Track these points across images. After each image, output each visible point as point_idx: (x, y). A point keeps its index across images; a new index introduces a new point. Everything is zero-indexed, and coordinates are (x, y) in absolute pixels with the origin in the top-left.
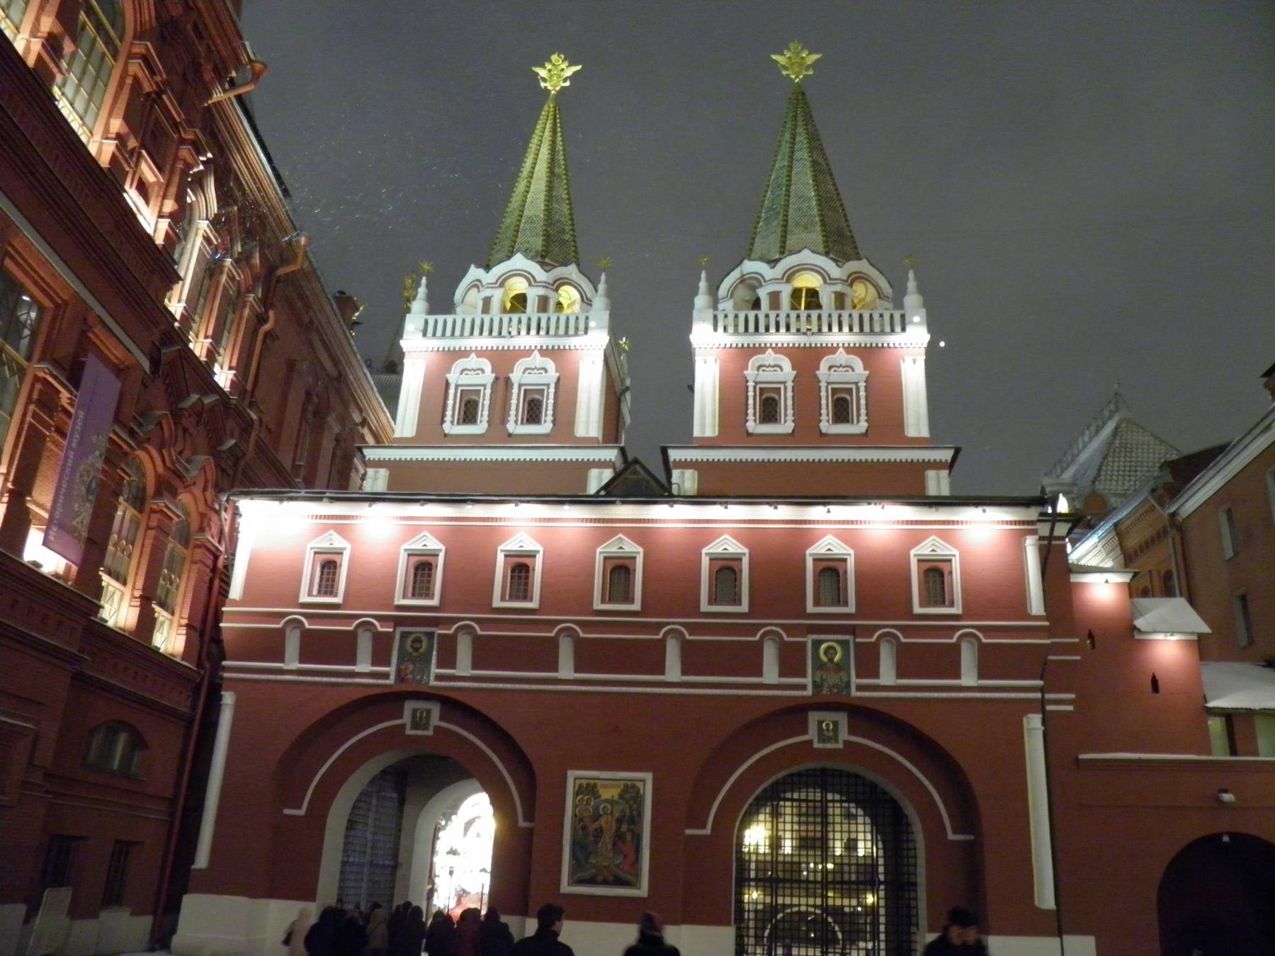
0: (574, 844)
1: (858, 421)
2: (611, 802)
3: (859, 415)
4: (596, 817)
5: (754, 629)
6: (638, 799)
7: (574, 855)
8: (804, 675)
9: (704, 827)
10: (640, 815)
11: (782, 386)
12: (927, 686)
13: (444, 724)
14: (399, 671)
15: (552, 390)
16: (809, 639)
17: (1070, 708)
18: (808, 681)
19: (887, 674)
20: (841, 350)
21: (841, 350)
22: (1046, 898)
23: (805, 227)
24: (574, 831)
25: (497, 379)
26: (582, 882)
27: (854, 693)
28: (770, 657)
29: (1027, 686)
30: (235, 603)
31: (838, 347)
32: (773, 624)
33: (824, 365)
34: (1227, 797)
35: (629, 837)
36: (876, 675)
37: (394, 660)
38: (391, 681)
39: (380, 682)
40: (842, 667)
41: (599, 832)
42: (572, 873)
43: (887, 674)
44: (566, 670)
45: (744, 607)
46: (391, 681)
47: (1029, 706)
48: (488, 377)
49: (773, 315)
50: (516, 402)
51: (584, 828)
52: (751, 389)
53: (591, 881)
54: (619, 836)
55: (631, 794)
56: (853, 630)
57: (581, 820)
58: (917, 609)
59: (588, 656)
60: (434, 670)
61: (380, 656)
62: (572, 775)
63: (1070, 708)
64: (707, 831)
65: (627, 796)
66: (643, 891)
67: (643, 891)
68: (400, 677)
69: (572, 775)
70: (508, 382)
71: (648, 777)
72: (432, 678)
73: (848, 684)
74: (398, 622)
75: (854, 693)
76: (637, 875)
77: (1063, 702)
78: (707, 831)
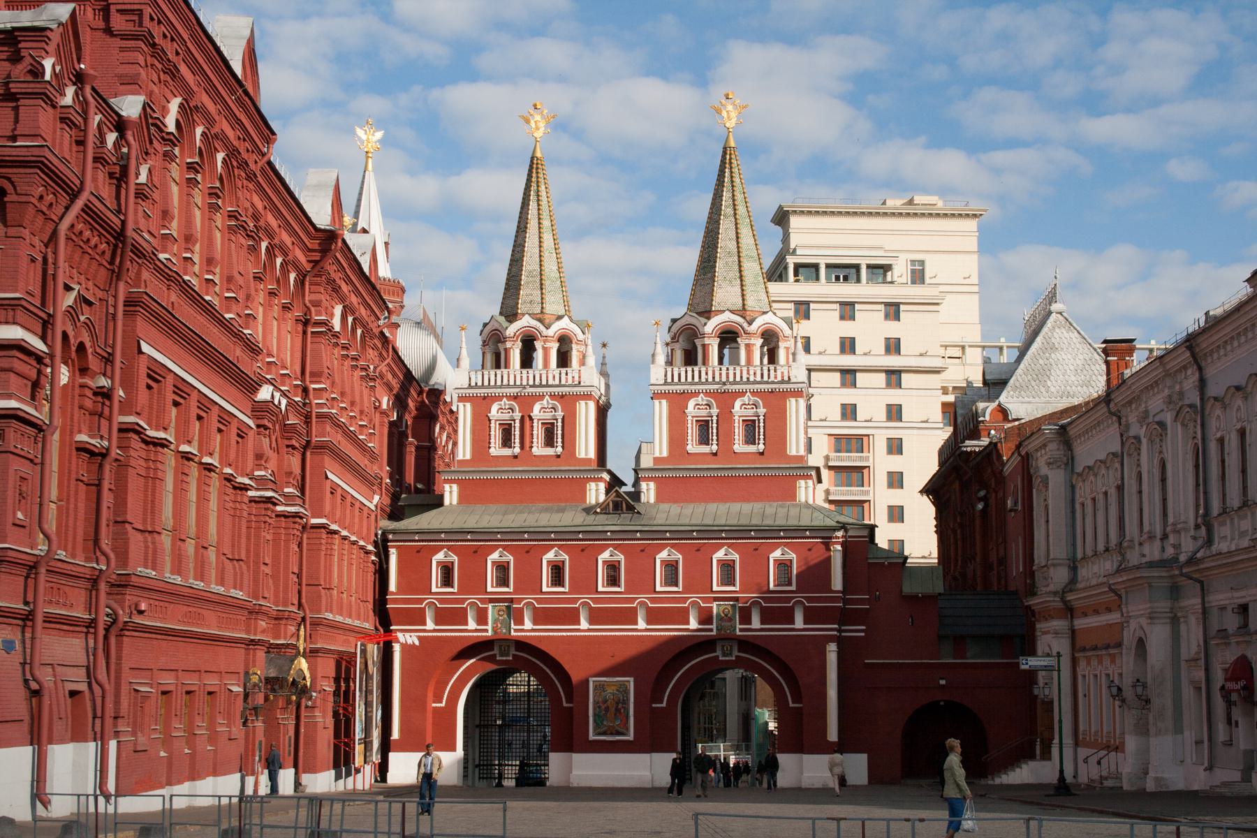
0: (595, 715)
2: (613, 694)
4: (605, 701)
5: (684, 600)
6: (627, 692)
7: (595, 721)
10: (628, 699)
12: (777, 630)
19: (756, 623)
22: (833, 735)
24: (594, 709)
26: (599, 734)
29: (831, 628)
30: (393, 593)
32: (694, 597)
33: (738, 403)
34: (943, 682)
40: (730, 620)
41: (607, 709)
42: (595, 730)
43: (756, 623)
44: (584, 624)
46: (490, 633)
47: (830, 639)
48: (517, 415)
49: (703, 369)
50: (538, 432)
53: (604, 733)
54: (617, 710)
55: (624, 689)
59: (595, 617)
61: (482, 618)
64: (664, 705)
66: (631, 737)
67: (631, 737)
70: (530, 417)
71: (631, 679)
74: (492, 600)
75: (738, 633)
76: (628, 729)
77: (857, 631)
78: (664, 705)
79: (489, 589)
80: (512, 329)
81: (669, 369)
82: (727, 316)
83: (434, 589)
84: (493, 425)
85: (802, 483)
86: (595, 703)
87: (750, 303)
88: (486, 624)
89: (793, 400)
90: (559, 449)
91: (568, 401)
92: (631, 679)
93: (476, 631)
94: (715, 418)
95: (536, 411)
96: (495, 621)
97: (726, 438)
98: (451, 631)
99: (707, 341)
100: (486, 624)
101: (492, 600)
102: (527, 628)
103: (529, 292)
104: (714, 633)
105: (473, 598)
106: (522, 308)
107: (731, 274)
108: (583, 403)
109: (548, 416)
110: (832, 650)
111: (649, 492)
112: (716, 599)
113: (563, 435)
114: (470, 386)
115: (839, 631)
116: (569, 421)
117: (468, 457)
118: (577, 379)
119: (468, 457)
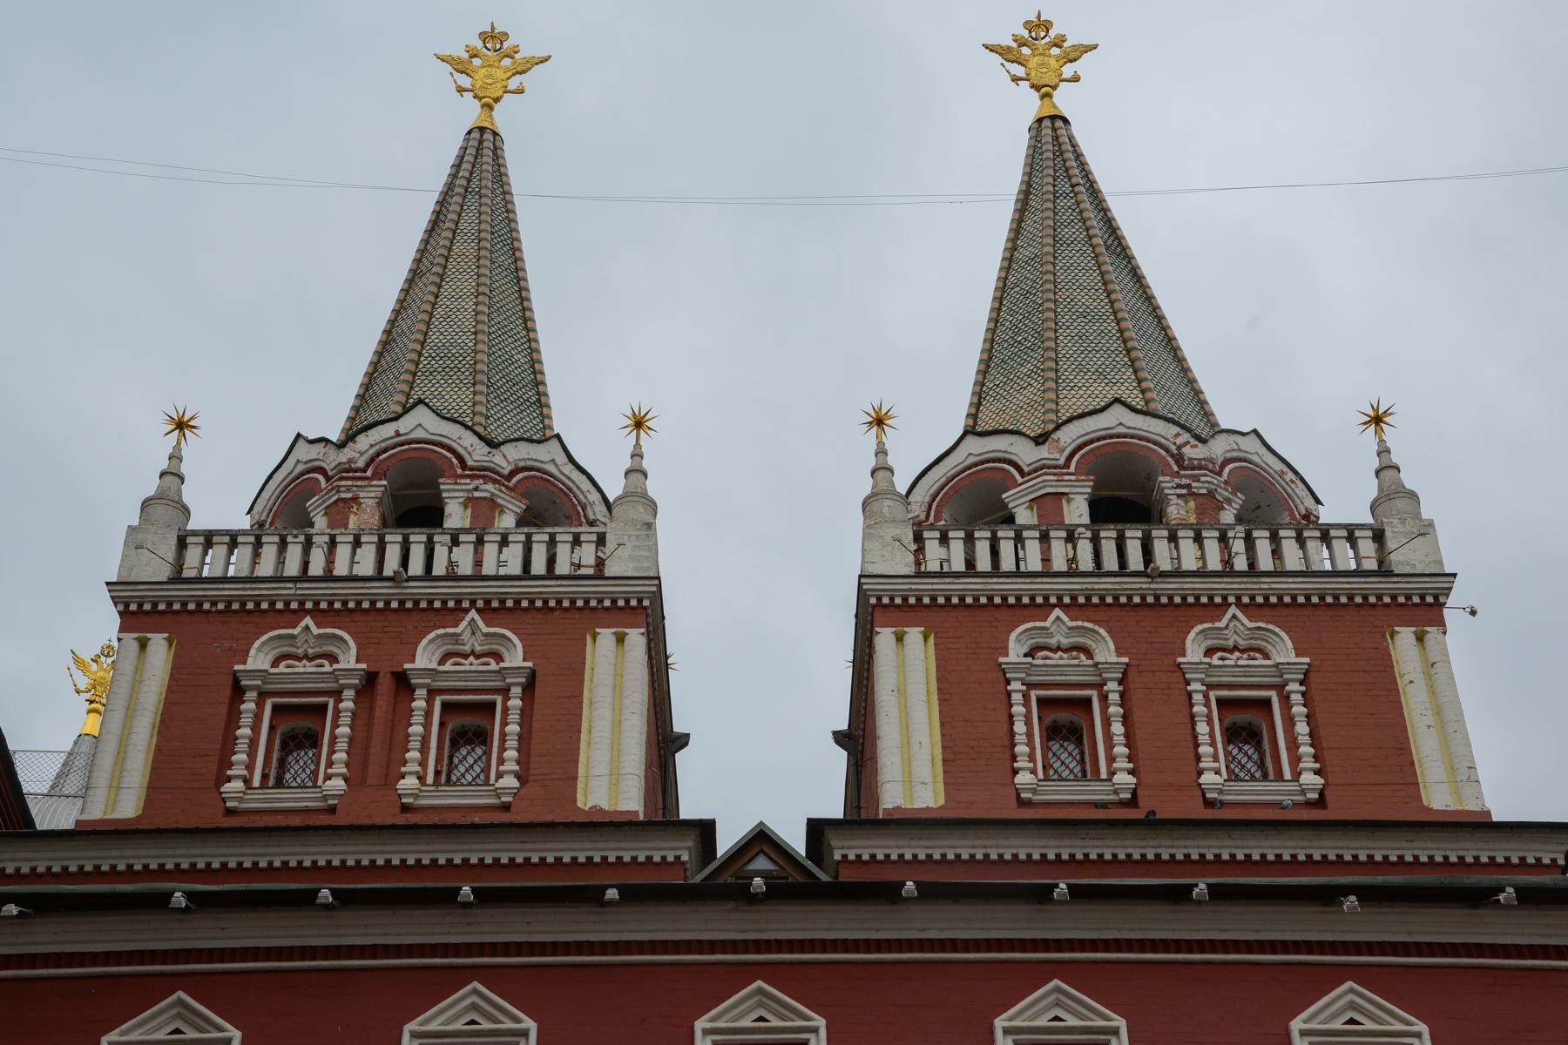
1: (1297, 775)
3: (1295, 759)
15: (515, 703)
25: (371, 678)
31: (1225, 605)
70: (403, 682)
84: (249, 706)
108: (606, 635)
113: (524, 740)
114: (177, 578)
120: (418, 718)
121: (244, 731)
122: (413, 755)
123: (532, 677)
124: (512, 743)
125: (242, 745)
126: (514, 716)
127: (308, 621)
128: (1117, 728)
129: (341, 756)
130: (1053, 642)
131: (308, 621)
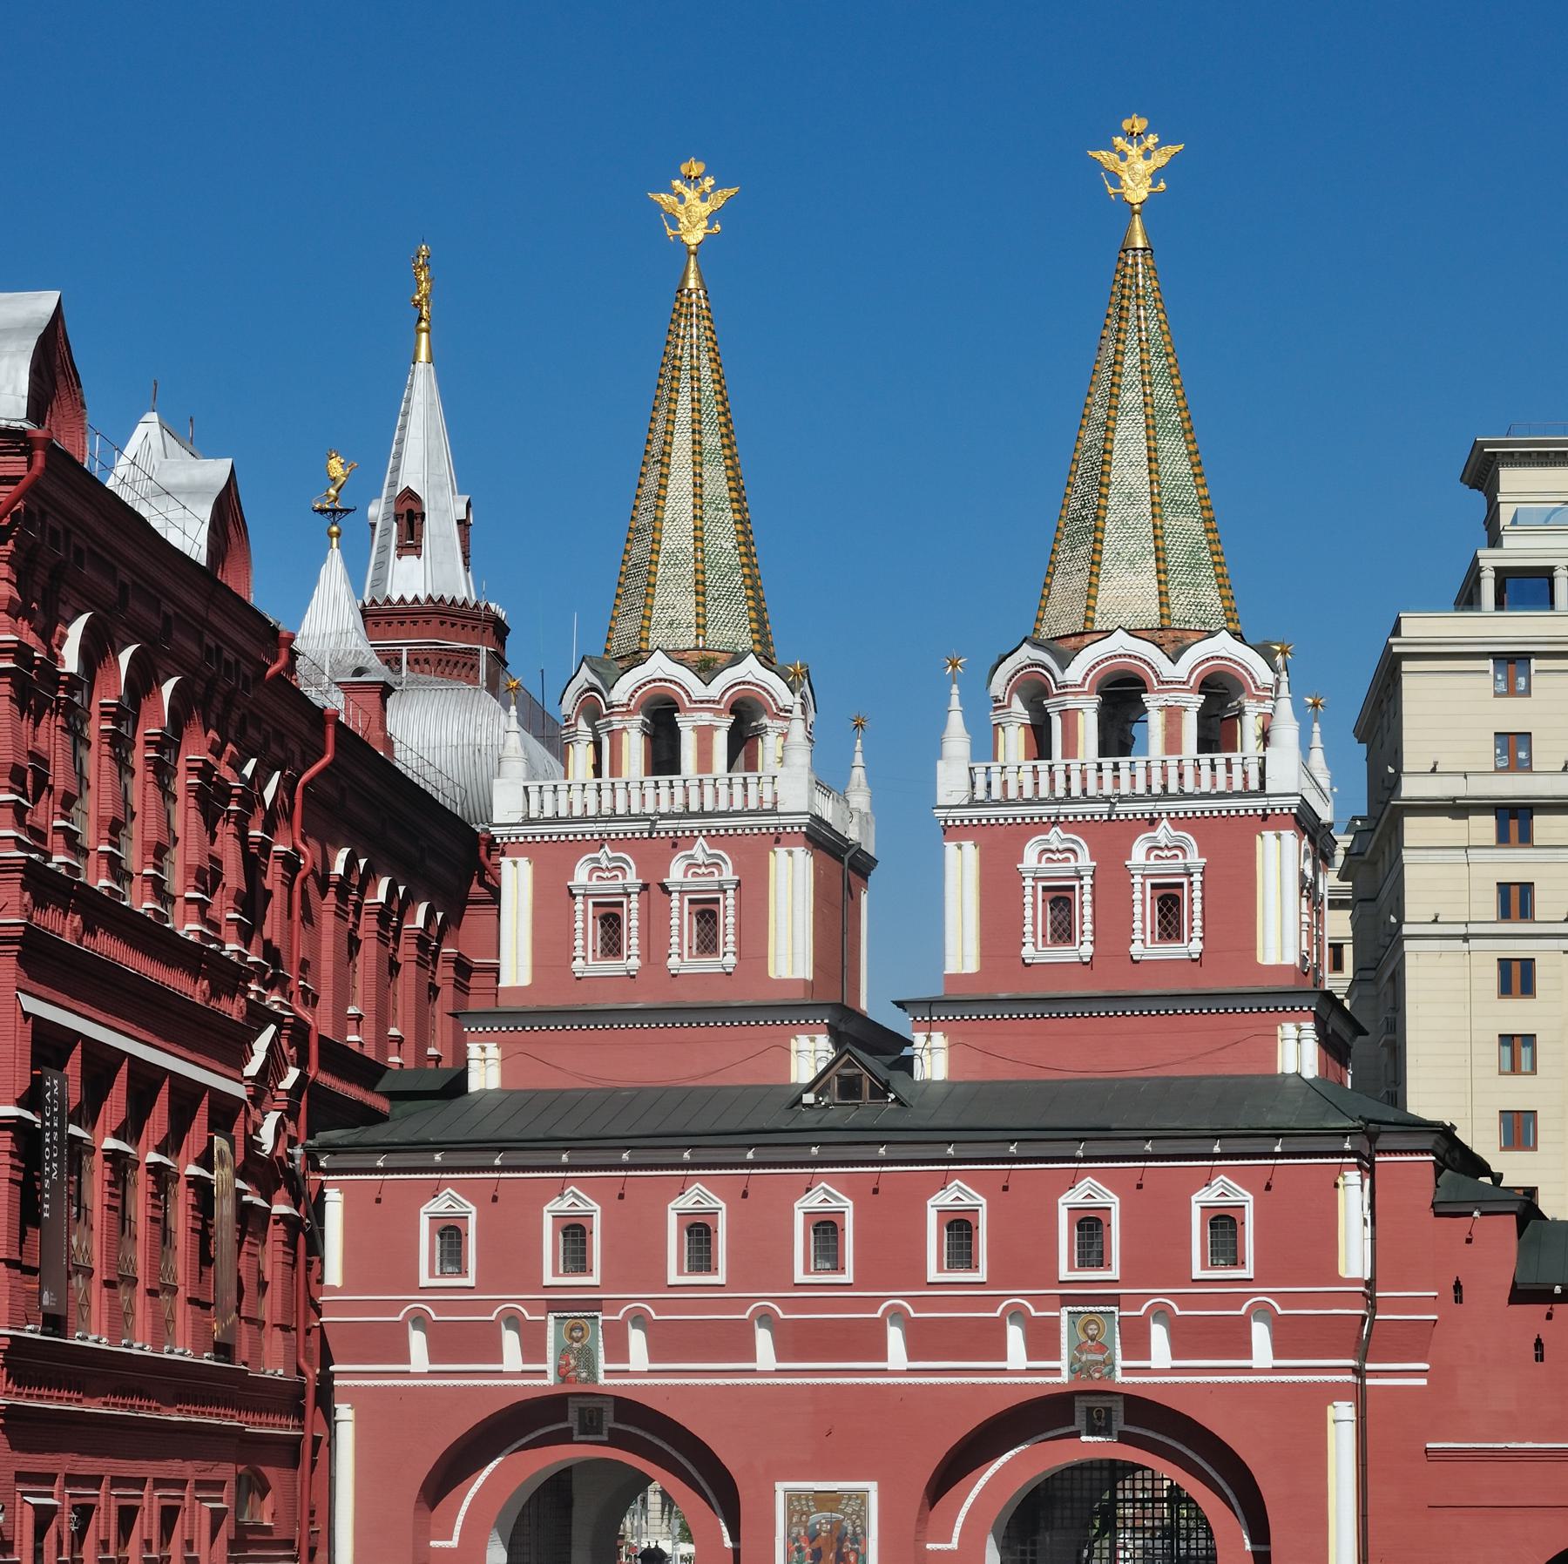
6: (862, 1514)
8: (1058, 1359)
9: (949, 1541)
10: (864, 1533)
11: (1076, 883)
13: (620, 1426)
14: (559, 1368)
15: (730, 902)
16: (1064, 1311)
17: (1423, 1382)
18: (1063, 1364)
20: (1165, 822)
21: (1165, 822)
23: (1131, 563)
24: (788, 1553)
25: (645, 887)
27: (1119, 1377)
28: (1015, 1336)
32: (1017, 1296)
35: (852, 1558)
36: (1147, 1356)
37: (550, 1354)
38: (550, 1380)
39: (536, 1382)
45: (981, 1275)
46: (550, 1380)
48: (632, 878)
51: (800, 1550)
52: (1028, 891)
56: (1114, 1300)
57: (797, 1539)
58: (1197, 1273)
59: (792, 1342)
60: (602, 1365)
61: (533, 1348)
62: (781, 1487)
63: (1423, 1382)
65: (849, 1510)
68: (562, 1373)
69: (781, 1487)
71: (872, 1487)
72: (601, 1375)
73: (1113, 1365)
74: (553, 1306)
75: (1119, 1377)
79: (548, 1279)
80: (622, 690)
81: (980, 770)
82: (1120, 642)
83: (425, 1280)
84: (579, 907)
85: (1289, 1029)
86: (791, 1538)
87: (1178, 610)
88: (544, 1360)
89: (1269, 835)
90: (731, 960)
91: (750, 847)
92: (872, 1487)
93: (525, 1374)
94: (1087, 881)
95: (676, 873)
96: (563, 1353)
97: (1114, 926)
98: (466, 1376)
99: (1071, 703)
100: (544, 1360)
101: (553, 1306)
102: (636, 1366)
103: (671, 600)
104: (1064, 1378)
105: (513, 1301)
106: (655, 638)
107: (1133, 547)
109: (705, 882)
110: (1341, 1421)
111: (933, 1060)
112: (1066, 1300)
114: (528, 821)
115: (1358, 1372)
116: (753, 888)
117: (525, 979)
118: (768, 797)
119: (525, 979)
120: (675, 913)
121: (579, 925)
122: (675, 940)
123: (739, 884)
124: (730, 930)
125: (579, 935)
126: (730, 912)
127: (607, 848)
128: (1088, 911)
129: (634, 941)
130: (1053, 847)
131: (607, 848)
